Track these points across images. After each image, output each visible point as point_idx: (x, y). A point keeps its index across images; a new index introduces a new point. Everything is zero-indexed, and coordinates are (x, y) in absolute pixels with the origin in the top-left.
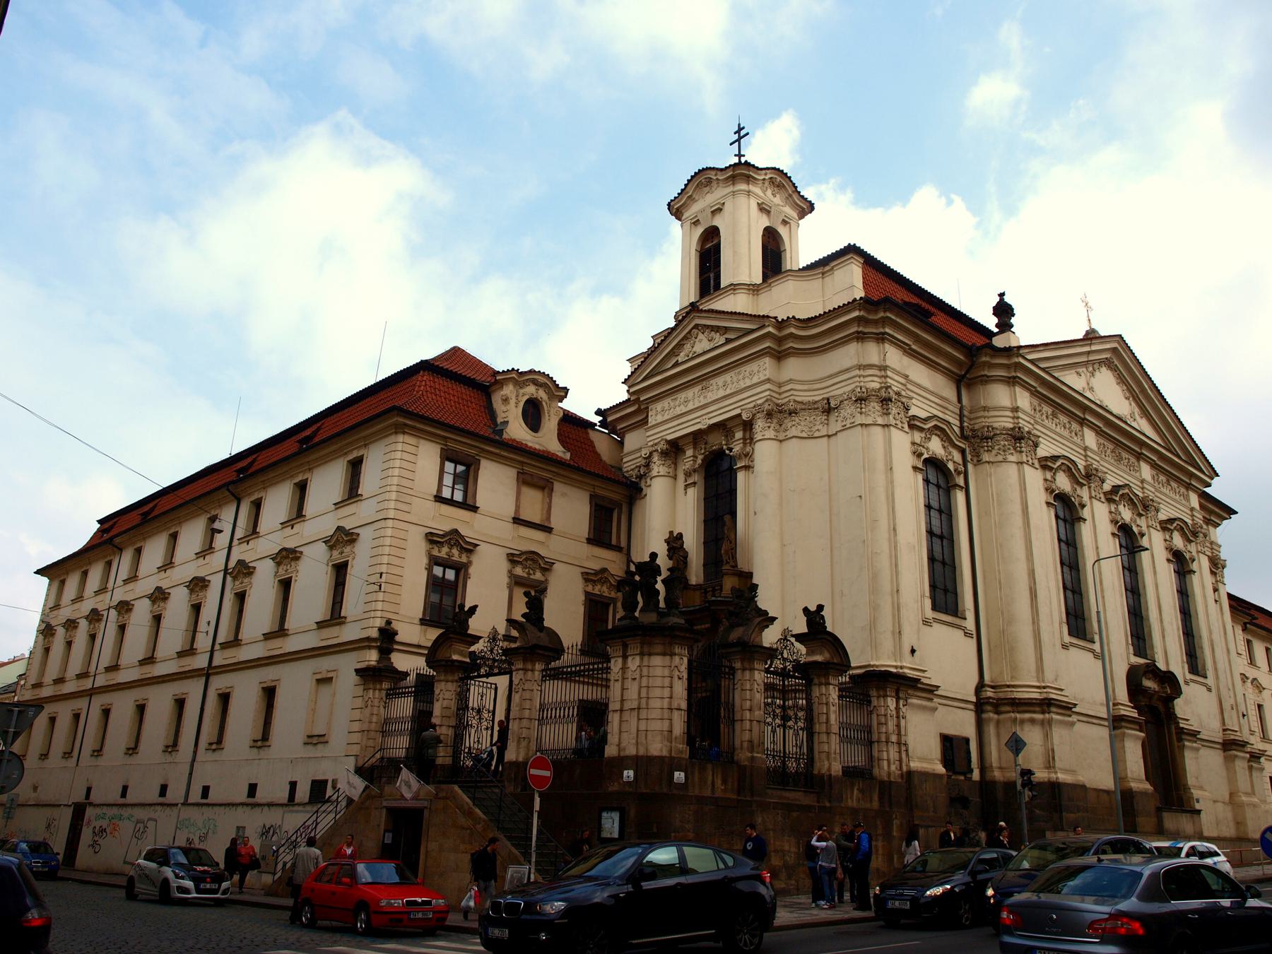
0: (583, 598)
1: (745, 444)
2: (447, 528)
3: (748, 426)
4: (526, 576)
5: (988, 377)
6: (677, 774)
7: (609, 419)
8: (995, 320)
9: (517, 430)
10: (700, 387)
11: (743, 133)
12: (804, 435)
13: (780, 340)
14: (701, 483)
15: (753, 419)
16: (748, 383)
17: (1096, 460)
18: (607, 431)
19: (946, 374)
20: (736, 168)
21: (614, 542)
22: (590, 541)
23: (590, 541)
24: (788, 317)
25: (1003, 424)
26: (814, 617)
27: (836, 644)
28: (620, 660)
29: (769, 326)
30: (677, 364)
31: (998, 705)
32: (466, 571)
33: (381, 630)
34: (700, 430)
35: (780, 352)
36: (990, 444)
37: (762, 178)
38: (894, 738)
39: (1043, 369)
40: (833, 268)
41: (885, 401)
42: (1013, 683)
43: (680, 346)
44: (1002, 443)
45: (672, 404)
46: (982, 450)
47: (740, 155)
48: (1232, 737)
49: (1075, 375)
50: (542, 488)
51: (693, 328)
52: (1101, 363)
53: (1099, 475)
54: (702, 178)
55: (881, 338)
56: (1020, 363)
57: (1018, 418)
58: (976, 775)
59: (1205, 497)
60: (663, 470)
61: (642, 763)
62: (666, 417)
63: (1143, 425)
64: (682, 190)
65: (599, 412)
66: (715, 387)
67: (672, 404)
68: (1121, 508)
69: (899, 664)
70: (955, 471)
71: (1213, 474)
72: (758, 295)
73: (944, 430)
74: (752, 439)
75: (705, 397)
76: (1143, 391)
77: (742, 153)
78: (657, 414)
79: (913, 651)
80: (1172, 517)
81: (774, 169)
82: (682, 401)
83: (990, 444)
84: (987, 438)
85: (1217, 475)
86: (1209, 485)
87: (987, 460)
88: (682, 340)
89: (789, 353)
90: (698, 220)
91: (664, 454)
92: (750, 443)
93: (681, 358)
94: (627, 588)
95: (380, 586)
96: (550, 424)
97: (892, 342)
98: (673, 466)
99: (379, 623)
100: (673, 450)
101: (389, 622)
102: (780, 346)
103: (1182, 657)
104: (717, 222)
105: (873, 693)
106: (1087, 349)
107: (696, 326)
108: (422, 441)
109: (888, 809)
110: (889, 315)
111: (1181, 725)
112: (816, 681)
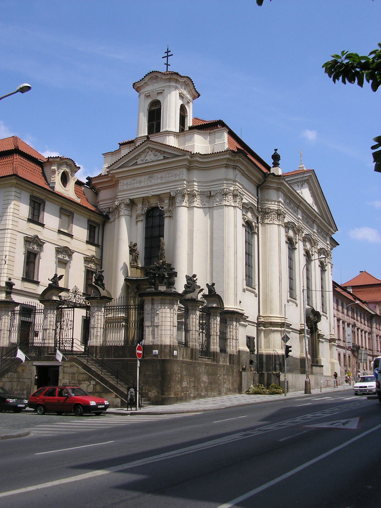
0: (84, 269)
1: (169, 206)
2: (32, 234)
3: (172, 199)
4: (62, 258)
5: (270, 186)
6: (175, 351)
7: (93, 182)
8: (272, 161)
9: (59, 188)
10: (148, 176)
11: (169, 54)
12: (198, 206)
13: (190, 162)
14: (144, 221)
15: (176, 196)
16: (174, 179)
17: (301, 223)
18: (89, 187)
19: (254, 183)
20: (172, 75)
21: (96, 242)
22: (88, 242)
23: (88, 242)
24: (196, 153)
25: (274, 208)
26: (211, 288)
27: (219, 299)
28: (150, 305)
29: (187, 155)
30: (136, 164)
31: (265, 324)
32: (40, 255)
33: (7, 283)
34: (148, 197)
35: (189, 167)
36: (268, 215)
37: (182, 81)
38: (235, 338)
39: (289, 184)
40: (215, 132)
41: (235, 196)
42: (269, 316)
43: (139, 155)
44: (273, 216)
45: (132, 181)
46: (265, 218)
47: (167, 65)
48: (333, 337)
49: (297, 186)
50: (69, 216)
51: (147, 148)
52: (305, 181)
53: (302, 230)
54: (153, 75)
55: (235, 168)
56: (283, 183)
57: (280, 205)
58: (256, 353)
59: (332, 239)
60: (126, 212)
61: (161, 348)
62: (129, 187)
63: (315, 208)
64: (143, 79)
65: (88, 178)
66: (156, 178)
67: (132, 182)
68: (307, 243)
69: (236, 307)
70: (255, 226)
71: (336, 230)
72: (178, 137)
73: (253, 209)
74: (172, 204)
75: (151, 181)
76: (318, 194)
77: (168, 64)
78: (123, 185)
79: (240, 302)
80: (322, 247)
81: (187, 77)
82: (138, 181)
83: (268, 215)
84: (267, 213)
85: (337, 230)
86: (334, 234)
87: (267, 222)
88: (140, 153)
89: (194, 168)
90: (150, 95)
91: (127, 205)
92: (172, 206)
93: (139, 162)
94: (152, 275)
95: (6, 261)
96: (71, 184)
97: (240, 171)
98: (130, 211)
99: (6, 279)
100: (132, 203)
101: (10, 279)
102: (190, 164)
103: (320, 306)
104: (159, 98)
105: (228, 319)
106: (302, 176)
107: (148, 148)
108: (23, 191)
109: (232, 365)
110: (240, 159)
111: (319, 333)
112: (212, 314)
